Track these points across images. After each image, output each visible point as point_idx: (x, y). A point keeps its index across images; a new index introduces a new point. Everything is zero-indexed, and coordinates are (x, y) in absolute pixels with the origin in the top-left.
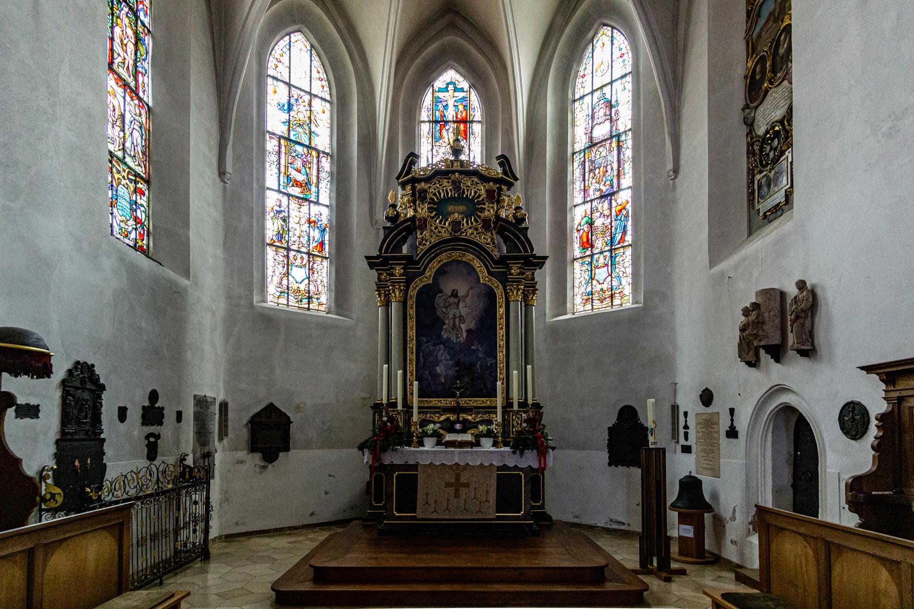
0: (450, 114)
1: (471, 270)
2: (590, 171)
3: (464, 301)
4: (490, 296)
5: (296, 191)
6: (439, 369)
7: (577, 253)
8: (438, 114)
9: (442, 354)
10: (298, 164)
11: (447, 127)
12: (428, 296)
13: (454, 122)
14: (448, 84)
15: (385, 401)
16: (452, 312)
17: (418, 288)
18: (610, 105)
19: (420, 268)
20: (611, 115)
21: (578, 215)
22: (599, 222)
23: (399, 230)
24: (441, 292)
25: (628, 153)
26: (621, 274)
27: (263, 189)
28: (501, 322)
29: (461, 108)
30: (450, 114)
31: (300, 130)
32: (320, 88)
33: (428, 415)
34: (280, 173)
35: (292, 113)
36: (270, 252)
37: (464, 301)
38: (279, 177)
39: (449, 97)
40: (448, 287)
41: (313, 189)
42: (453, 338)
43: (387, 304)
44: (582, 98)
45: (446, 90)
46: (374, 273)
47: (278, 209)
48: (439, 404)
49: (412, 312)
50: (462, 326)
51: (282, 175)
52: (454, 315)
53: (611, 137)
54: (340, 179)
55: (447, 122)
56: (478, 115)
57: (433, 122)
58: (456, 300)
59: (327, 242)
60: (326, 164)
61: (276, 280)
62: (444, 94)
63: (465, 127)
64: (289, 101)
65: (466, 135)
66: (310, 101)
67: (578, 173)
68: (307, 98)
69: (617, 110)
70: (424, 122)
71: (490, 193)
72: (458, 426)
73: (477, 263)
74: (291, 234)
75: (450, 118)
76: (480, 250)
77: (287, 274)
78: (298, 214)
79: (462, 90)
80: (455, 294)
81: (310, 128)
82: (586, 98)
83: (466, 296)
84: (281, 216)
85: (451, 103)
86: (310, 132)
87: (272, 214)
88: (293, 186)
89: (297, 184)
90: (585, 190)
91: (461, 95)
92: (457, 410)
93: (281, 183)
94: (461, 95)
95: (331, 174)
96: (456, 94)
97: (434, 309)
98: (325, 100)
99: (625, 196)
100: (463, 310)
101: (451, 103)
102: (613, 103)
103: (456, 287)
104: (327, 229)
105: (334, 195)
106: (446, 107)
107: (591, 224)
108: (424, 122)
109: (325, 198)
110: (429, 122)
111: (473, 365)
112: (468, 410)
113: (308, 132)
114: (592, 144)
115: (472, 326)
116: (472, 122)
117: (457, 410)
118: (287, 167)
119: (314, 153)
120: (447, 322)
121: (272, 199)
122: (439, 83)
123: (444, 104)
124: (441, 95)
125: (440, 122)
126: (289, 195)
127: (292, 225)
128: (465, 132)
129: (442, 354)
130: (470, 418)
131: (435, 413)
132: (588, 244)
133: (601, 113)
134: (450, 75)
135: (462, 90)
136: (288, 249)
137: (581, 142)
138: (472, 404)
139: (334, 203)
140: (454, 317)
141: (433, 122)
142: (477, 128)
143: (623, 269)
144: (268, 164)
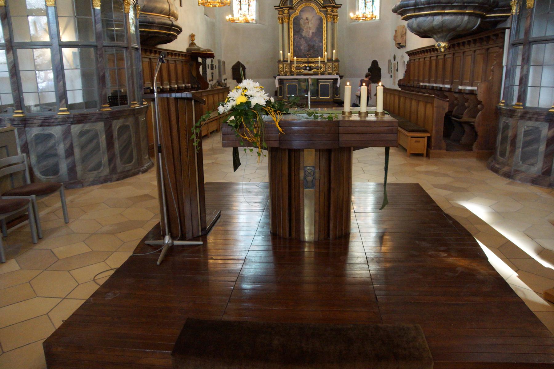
4: (321, 20)
6: (301, 47)
9: (303, 42)
15: (282, 60)
28: (324, 30)
40: (305, 16)
43: (282, 23)
46: (277, 11)
49: (291, 26)
72: (308, 68)
73: (316, 7)
80: (307, 19)
92: (308, 62)
100: (310, 25)
111: (314, 46)
112: (313, 63)
115: (314, 31)
117: (308, 62)
129: (303, 42)
130: (313, 65)
138: (314, 60)
140: (307, 28)
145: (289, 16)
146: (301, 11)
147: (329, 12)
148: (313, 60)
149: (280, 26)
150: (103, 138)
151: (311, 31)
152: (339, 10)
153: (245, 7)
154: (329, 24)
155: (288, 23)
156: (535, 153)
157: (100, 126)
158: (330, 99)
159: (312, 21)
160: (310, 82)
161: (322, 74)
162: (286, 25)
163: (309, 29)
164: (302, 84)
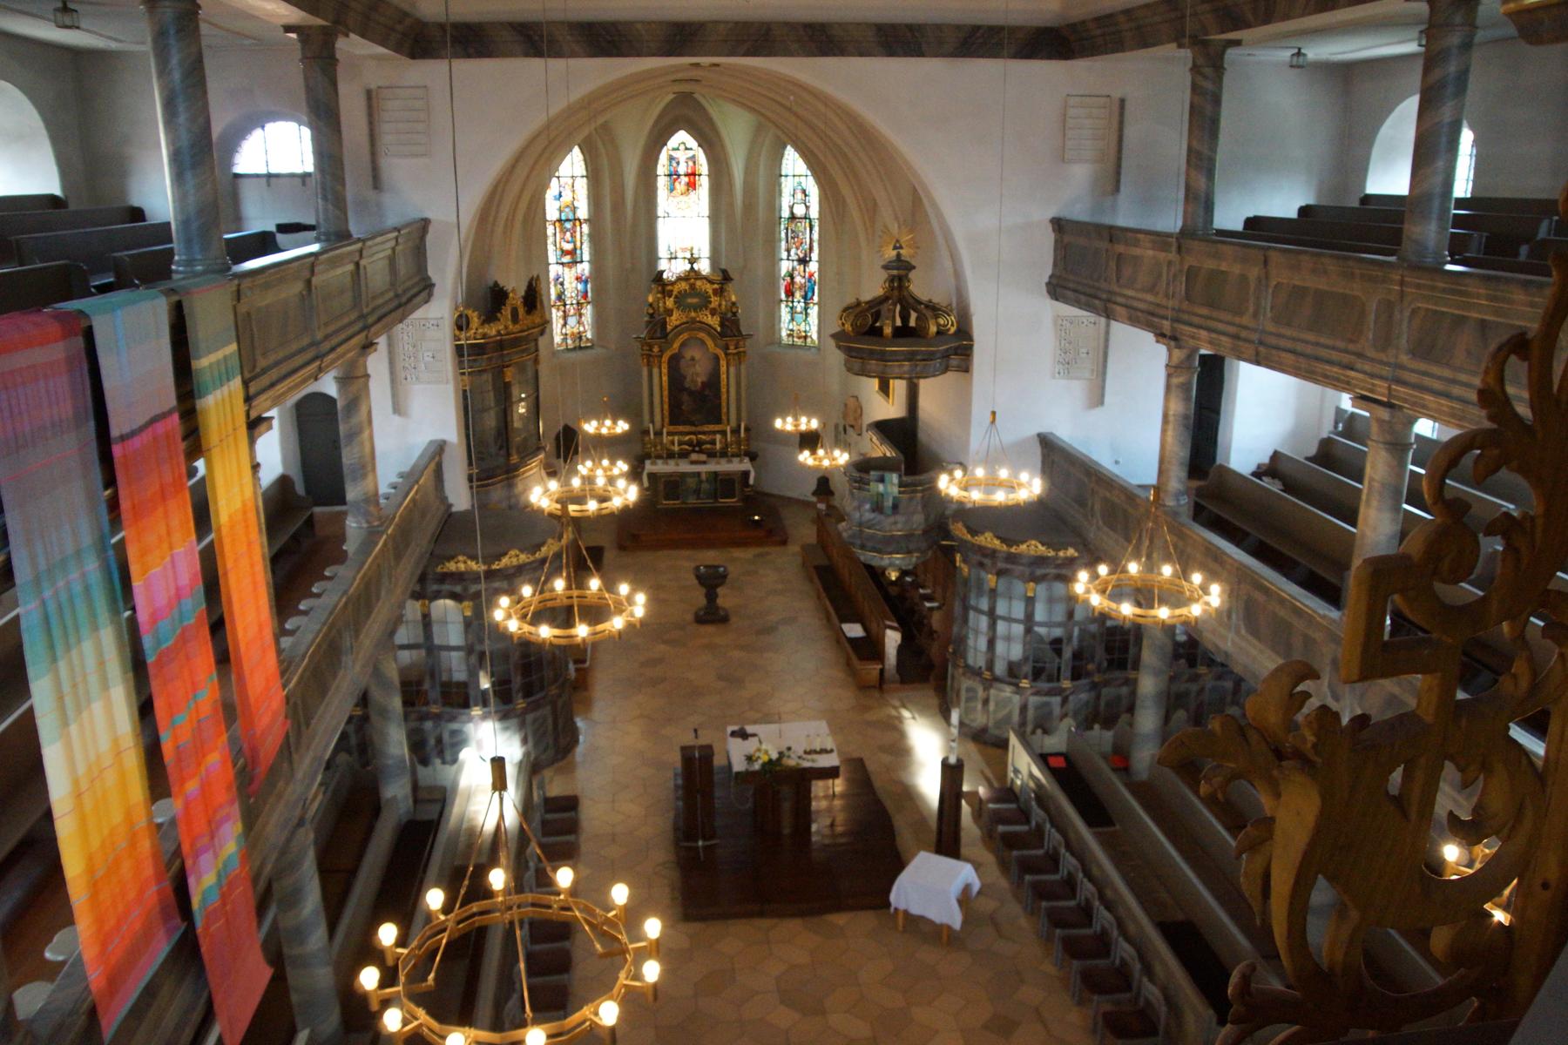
0: (682, 169)
1: (703, 343)
4: (717, 358)
5: (567, 259)
7: (783, 296)
9: (685, 397)
16: (691, 370)
18: (804, 192)
21: (785, 266)
22: (798, 279)
23: (657, 326)
25: (816, 236)
30: (682, 169)
39: (682, 156)
40: (689, 353)
49: (665, 371)
54: (595, 238)
56: (703, 167)
60: (586, 228)
67: (783, 235)
71: (715, 292)
76: (708, 328)
77: (565, 325)
78: (569, 276)
80: (693, 359)
90: (788, 251)
94: (690, 153)
95: (590, 235)
99: (813, 267)
100: (698, 369)
107: (792, 276)
109: (586, 257)
112: (704, 433)
114: (793, 217)
121: (554, 270)
122: (674, 141)
124: (674, 154)
125: (673, 175)
129: (685, 397)
132: (790, 293)
133: (799, 196)
137: (786, 213)
142: (704, 182)
146: (683, 345)
147: (732, 350)
148: (706, 428)
150: (550, 721)
151: (699, 380)
152: (748, 342)
153: (572, 321)
154: (732, 370)
156: (974, 709)
157: (547, 711)
160: (704, 477)
161: (724, 454)
162: (655, 371)
163: (697, 373)
164: (690, 480)
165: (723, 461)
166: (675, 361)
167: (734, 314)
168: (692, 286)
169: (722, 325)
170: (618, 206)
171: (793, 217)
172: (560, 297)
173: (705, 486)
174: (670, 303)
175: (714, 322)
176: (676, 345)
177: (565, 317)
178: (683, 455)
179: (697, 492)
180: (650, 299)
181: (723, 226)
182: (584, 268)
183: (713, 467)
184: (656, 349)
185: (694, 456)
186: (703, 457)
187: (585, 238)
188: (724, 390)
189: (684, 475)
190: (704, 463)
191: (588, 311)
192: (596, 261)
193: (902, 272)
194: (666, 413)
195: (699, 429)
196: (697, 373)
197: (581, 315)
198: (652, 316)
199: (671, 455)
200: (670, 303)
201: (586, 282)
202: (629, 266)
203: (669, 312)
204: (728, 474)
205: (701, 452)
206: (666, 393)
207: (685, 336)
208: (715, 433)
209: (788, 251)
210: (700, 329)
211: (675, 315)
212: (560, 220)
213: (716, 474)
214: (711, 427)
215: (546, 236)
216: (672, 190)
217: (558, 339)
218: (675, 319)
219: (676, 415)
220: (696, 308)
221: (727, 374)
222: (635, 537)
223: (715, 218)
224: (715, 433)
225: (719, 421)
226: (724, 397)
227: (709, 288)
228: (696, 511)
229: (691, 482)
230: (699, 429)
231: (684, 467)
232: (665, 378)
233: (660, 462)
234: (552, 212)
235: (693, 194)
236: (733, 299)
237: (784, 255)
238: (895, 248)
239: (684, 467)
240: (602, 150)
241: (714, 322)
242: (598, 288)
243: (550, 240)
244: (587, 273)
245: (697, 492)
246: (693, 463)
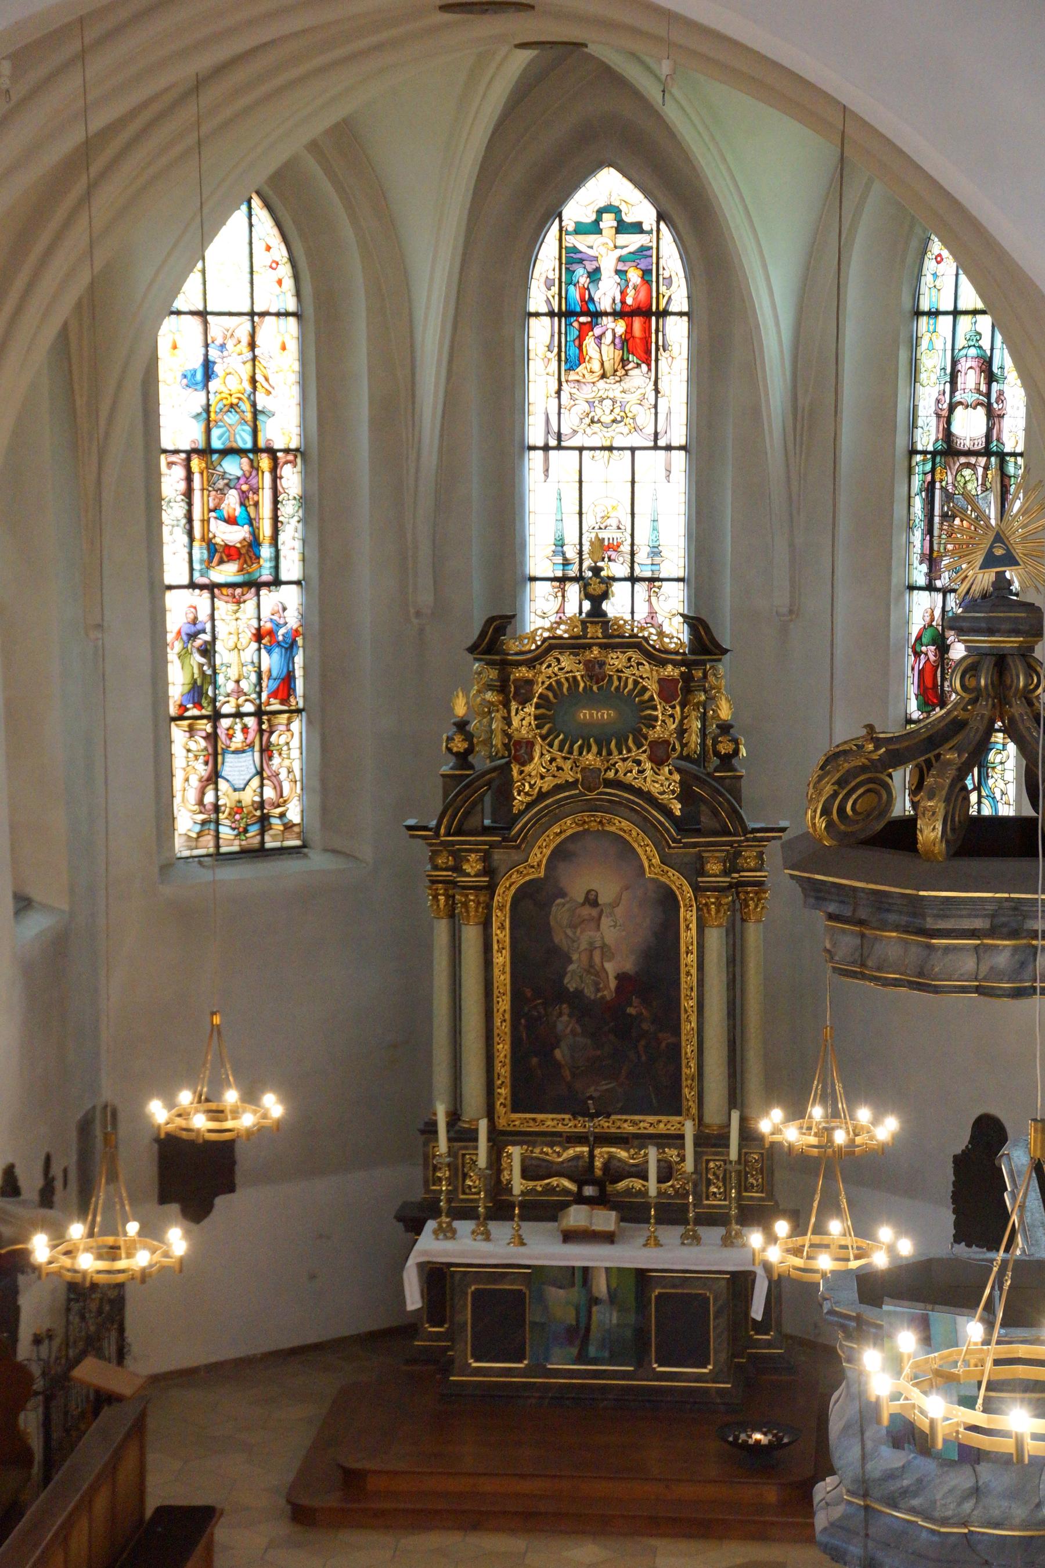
0: (606, 294)
1: (626, 850)
2: (944, 516)
3: (611, 914)
4: (668, 901)
5: (227, 572)
6: (558, 1054)
8: (574, 294)
9: (564, 1022)
10: (232, 499)
11: (597, 331)
12: (534, 903)
13: (616, 314)
14: (600, 212)
16: (586, 937)
17: (513, 890)
19: (518, 847)
20: (988, 395)
24: (562, 894)
26: (998, 796)
27: (158, 589)
29: (634, 276)
30: (606, 294)
31: (231, 418)
32: (277, 291)
33: (537, 1150)
34: (192, 539)
35: (213, 385)
36: (178, 734)
37: (611, 914)
38: (190, 554)
39: (605, 250)
41: (266, 552)
42: (589, 992)
44: (935, 314)
45: (595, 228)
46: (421, 850)
47: (193, 629)
48: (560, 1128)
49: (501, 935)
50: (607, 965)
51: (196, 544)
52: (591, 944)
53: (987, 452)
55: (598, 315)
57: (560, 315)
58: (594, 912)
59: (299, 673)
60: (291, 479)
61: (192, 795)
62: (591, 239)
63: (646, 329)
64: (206, 355)
65: (648, 352)
66: (253, 335)
68: (243, 326)
69: (1001, 393)
70: (537, 315)
71: (667, 689)
74: (220, 679)
75: (605, 305)
77: (214, 777)
78: (234, 625)
79: (637, 228)
81: (254, 405)
82: (941, 318)
83: (615, 904)
84: (198, 643)
85: (608, 264)
86: (256, 413)
87: (178, 646)
88: (221, 562)
89: (229, 553)
91: (633, 242)
93: (197, 566)
94: (633, 242)
95: (304, 500)
96: (623, 239)
97: (547, 930)
98: (287, 314)
100: (609, 932)
101: (608, 264)
102: (995, 369)
103: (594, 886)
104: (300, 641)
105: (314, 556)
106: (595, 275)
108: (537, 315)
109: (291, 568)
110: (551, 314)
113: (249, 416)
116: (665, 313)
118: (205, 522)
119: (265, 462)
120: (575, 957)
121: (180, 608)
122: (578, 208)
123: (590, 266)
124: (581, 242)
125: (577, 316)
126: (212, 588)
127: (223, 654)
128: (646, 341)
129: (564, 1022)
130: (623, 1154)
131: (551, 1145)
133: (970, 379)
134: (608, 187)
135: (637, 228)
136: (216, 716)
137: (927, 438)
138: (628, 1129)
139: (314, 573)
141: (560, 315)
142: (676, 332)
143: (1001, 784)
144: (166, 530)
145: (491, 889)
146: (560, 854)
148: (626, 1124)
149: (442, 929)
151: (611, 968)
153: (238, 768)
155: (486, 925)
158: (714, 1377)
159: (619, 911)
163: (605, 945)
164: (556, 1295)
165: (670, 1234)
166: (534, 903)
167: (727, 761)
168: (595, 671)
169: (686, 796)
170: (394, 408)
171: (949, 449)
172: (200, 690)
173: (605, 1318)
174: (523, 720)
175: (663, 783)
176: (539, 854)
177: (215, 754)
178: (542, 1210)
179: (579, 1335)
180: (460, 709)
181: (728, 477)
182: (285, 605)
183: (633, 1253)
184: (472, 866)
185: (576, 1216)
186: (605, 1220)
187: (289, 509)
188: (689, 1004)
189: (538, 1275)
190: (609, 1238)
191: (292, 739)
192: (325, 581)
193: (1011, 642)
194: (503, 1070)
195: (605, 1125)
196: (605, 945)
197: (266, 751)
198: (463, 758)
199: (501, 1208)
200: (523, 720)
201: (290, 648)
202: (425, 599)
203: (519, 751)
204: (686, 1278)
205: (601, 1201)
206: (503, 1005)
207: (569, 826)
208: (642, 1140)
209: (932, 560)
210: (613, 807)
211: (535, 767)
212: (206, 452)
213: (642, 1276)
214: (647, 1123)
215: (153, 501)
216: (569, 359)
217: (186, 821)
218: (538, 773)
219: (534, 1080)
220: (603, 740)
221: (700, 947)
222: (352, 1480)
223: (705, 451)
224: (642, 1140)
225: (673, 1105)
226: (688, 1026)
227: (650, 677)
228: (579, 1403)
229: (561, 1302)
230: (605, 1125)
231: (541, 1248)
232: (502, 959)
233: (464, 1227)
234: (178, 425)
235: (638, 378)
236: (725, 712)
237: (919, 574)
238: (990, 561)
239: (541, 1248)
240: (348, 233)
241: (663, 783)
242: (325, 675)
243: (173, 514)
244: (292, 619)
245: (579, 1335)
246: (569, 1236)
